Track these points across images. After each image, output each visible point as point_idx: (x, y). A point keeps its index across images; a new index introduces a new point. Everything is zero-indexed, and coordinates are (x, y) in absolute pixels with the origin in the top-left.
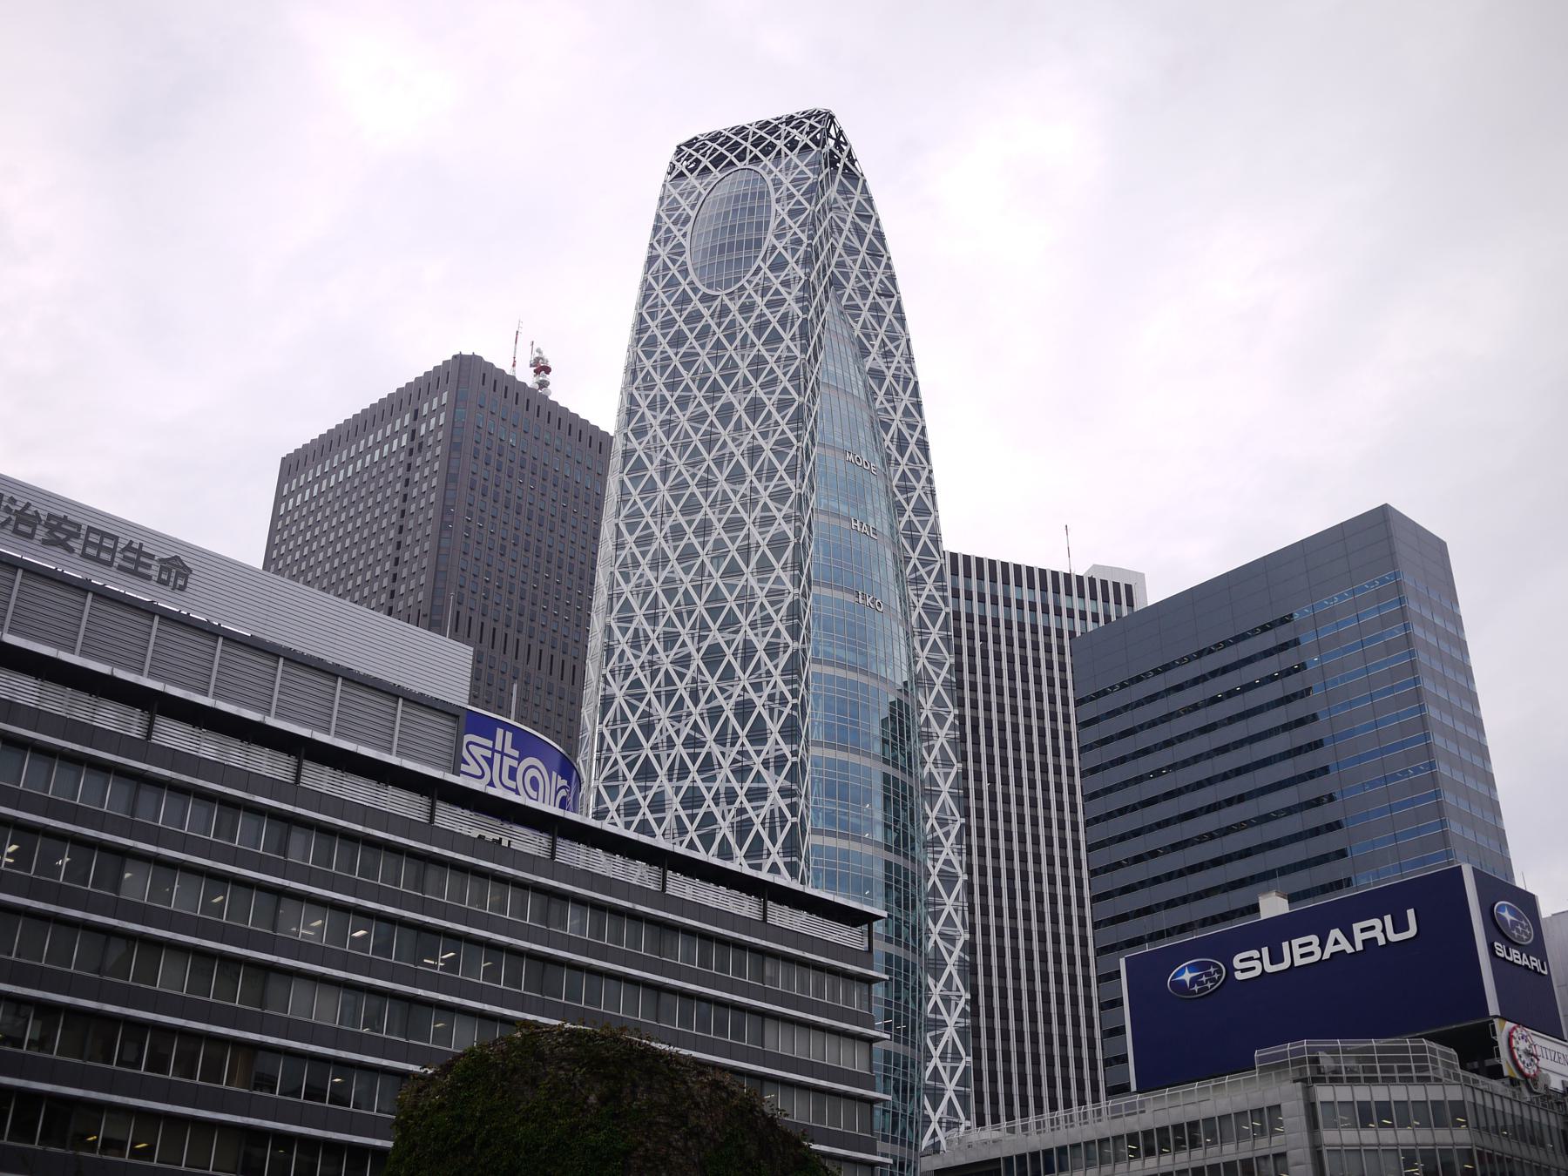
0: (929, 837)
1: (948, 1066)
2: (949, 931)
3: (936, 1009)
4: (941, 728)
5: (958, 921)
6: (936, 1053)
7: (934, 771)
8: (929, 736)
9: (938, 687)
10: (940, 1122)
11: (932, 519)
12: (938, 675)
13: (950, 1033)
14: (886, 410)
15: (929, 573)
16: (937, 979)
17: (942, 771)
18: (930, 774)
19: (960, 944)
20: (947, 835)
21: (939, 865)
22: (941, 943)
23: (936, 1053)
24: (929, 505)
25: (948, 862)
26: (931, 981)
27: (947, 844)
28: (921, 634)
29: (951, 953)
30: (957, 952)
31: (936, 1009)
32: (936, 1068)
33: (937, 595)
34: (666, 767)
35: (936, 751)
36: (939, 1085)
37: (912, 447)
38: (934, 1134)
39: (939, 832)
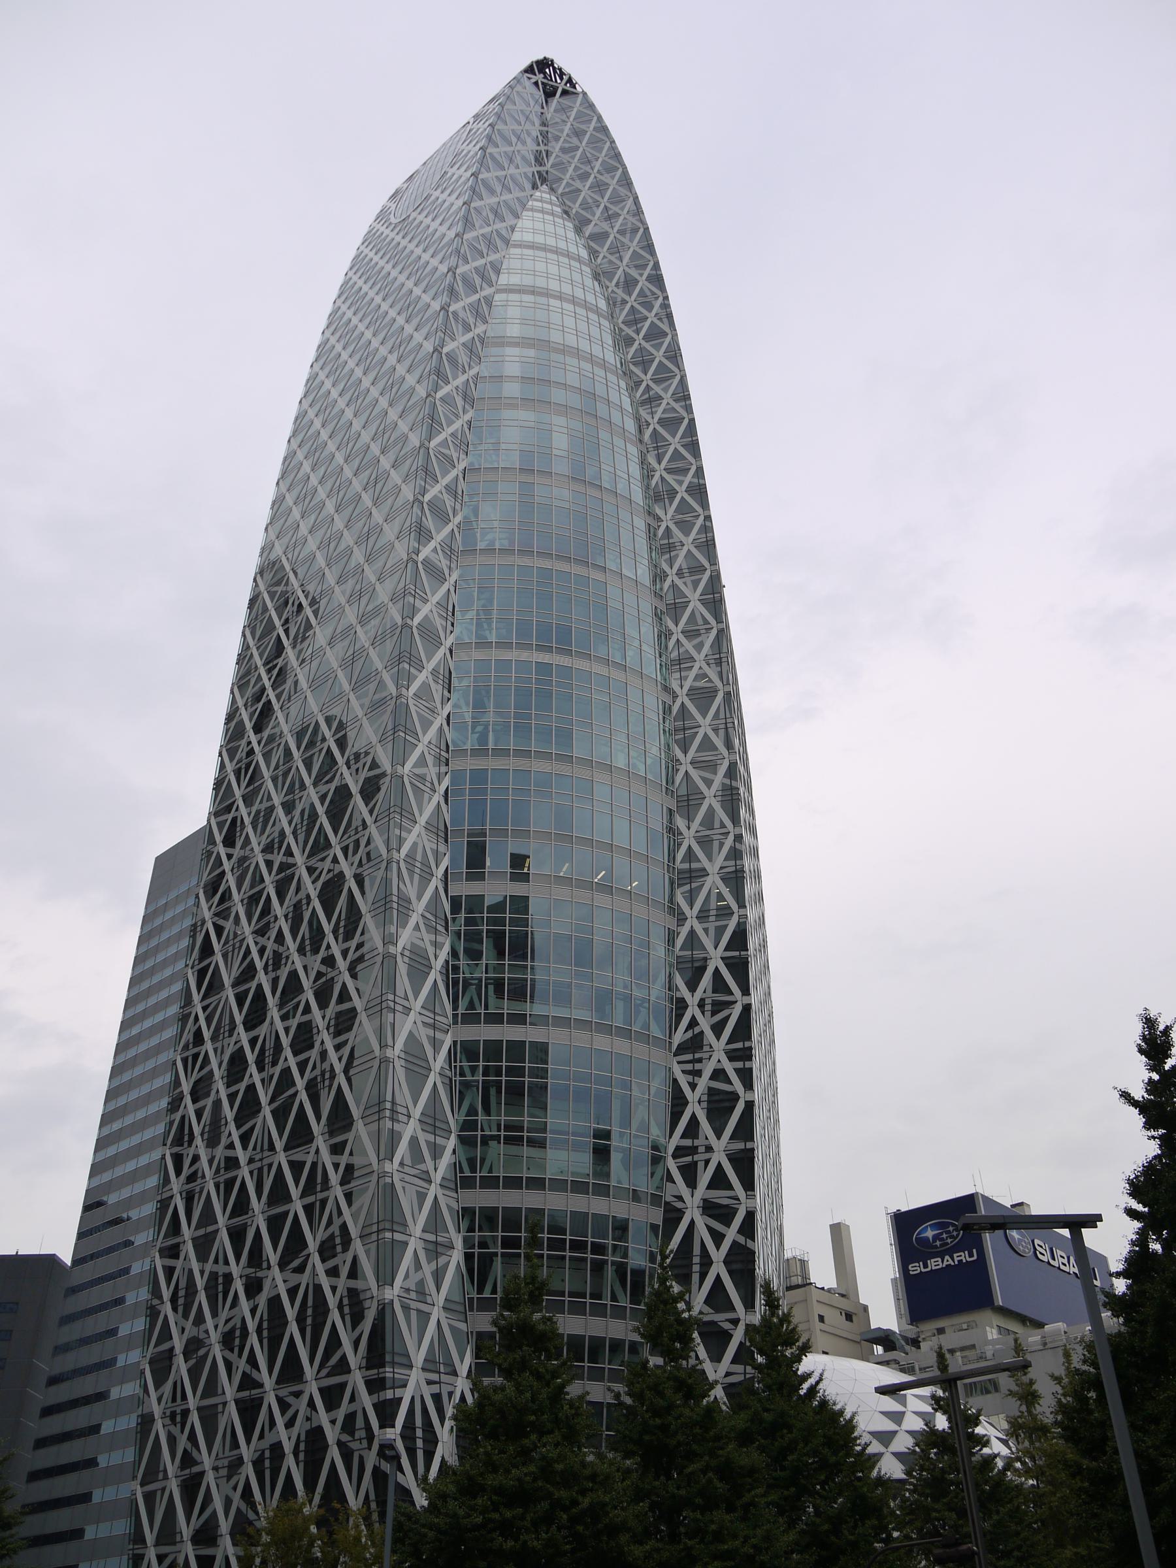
0: (674, 655)
1: (712, 927)
2: (707, 756)
3: (690, 855)
4: (687, 534)
5: (719, 742)
6: (691, 913)
7: (678, 582)
8: (670, 548)
9: (682, 492)
10: (701, 1005)
11: (668, 339)
12: (680, 483)
13: (713, 882)
14: (610, 262)
15: (666, 390)
16: (690, 819)
17: (688, 580)
18: (673, 585)
19: (723, 769)
20: (698, 648)
21: (687, 684)
22: (694, 774)
23: (691, 913)
24: (665, 327)
25: (702, 676)
26: (680, 823)
27: (700, 657)
28: (657, 448)
29: (709, 783)
30: (719, 779)
31: (690, 855)
32: (692, 932)
33: (677, 406)
34: (291, 638)
35: (680, 561)
36: (698, 954)
37: (642, 282)
38: (693, 1023)
39: (688, 645)
